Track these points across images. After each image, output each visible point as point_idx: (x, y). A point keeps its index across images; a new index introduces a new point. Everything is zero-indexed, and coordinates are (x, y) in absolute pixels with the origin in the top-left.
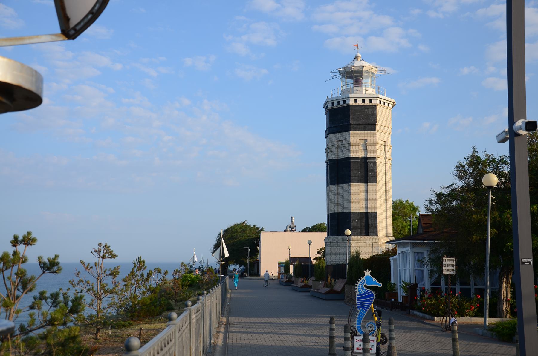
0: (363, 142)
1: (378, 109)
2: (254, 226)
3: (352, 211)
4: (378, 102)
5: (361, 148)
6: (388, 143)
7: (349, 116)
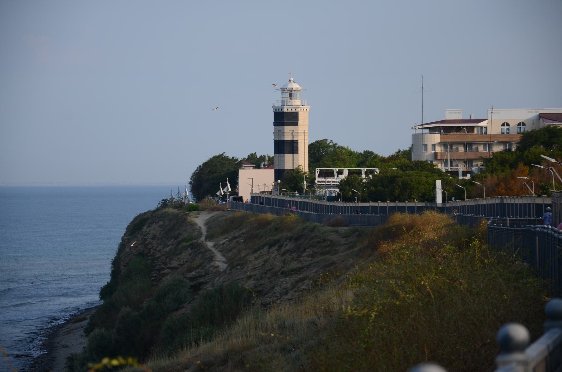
0: (291, 132)
1: (299, 113)
2: (233, 158)
3: (285, 168)
4: (300, 110)
5: (291, 135)
6: (306, 131)
7: (284, 118)
